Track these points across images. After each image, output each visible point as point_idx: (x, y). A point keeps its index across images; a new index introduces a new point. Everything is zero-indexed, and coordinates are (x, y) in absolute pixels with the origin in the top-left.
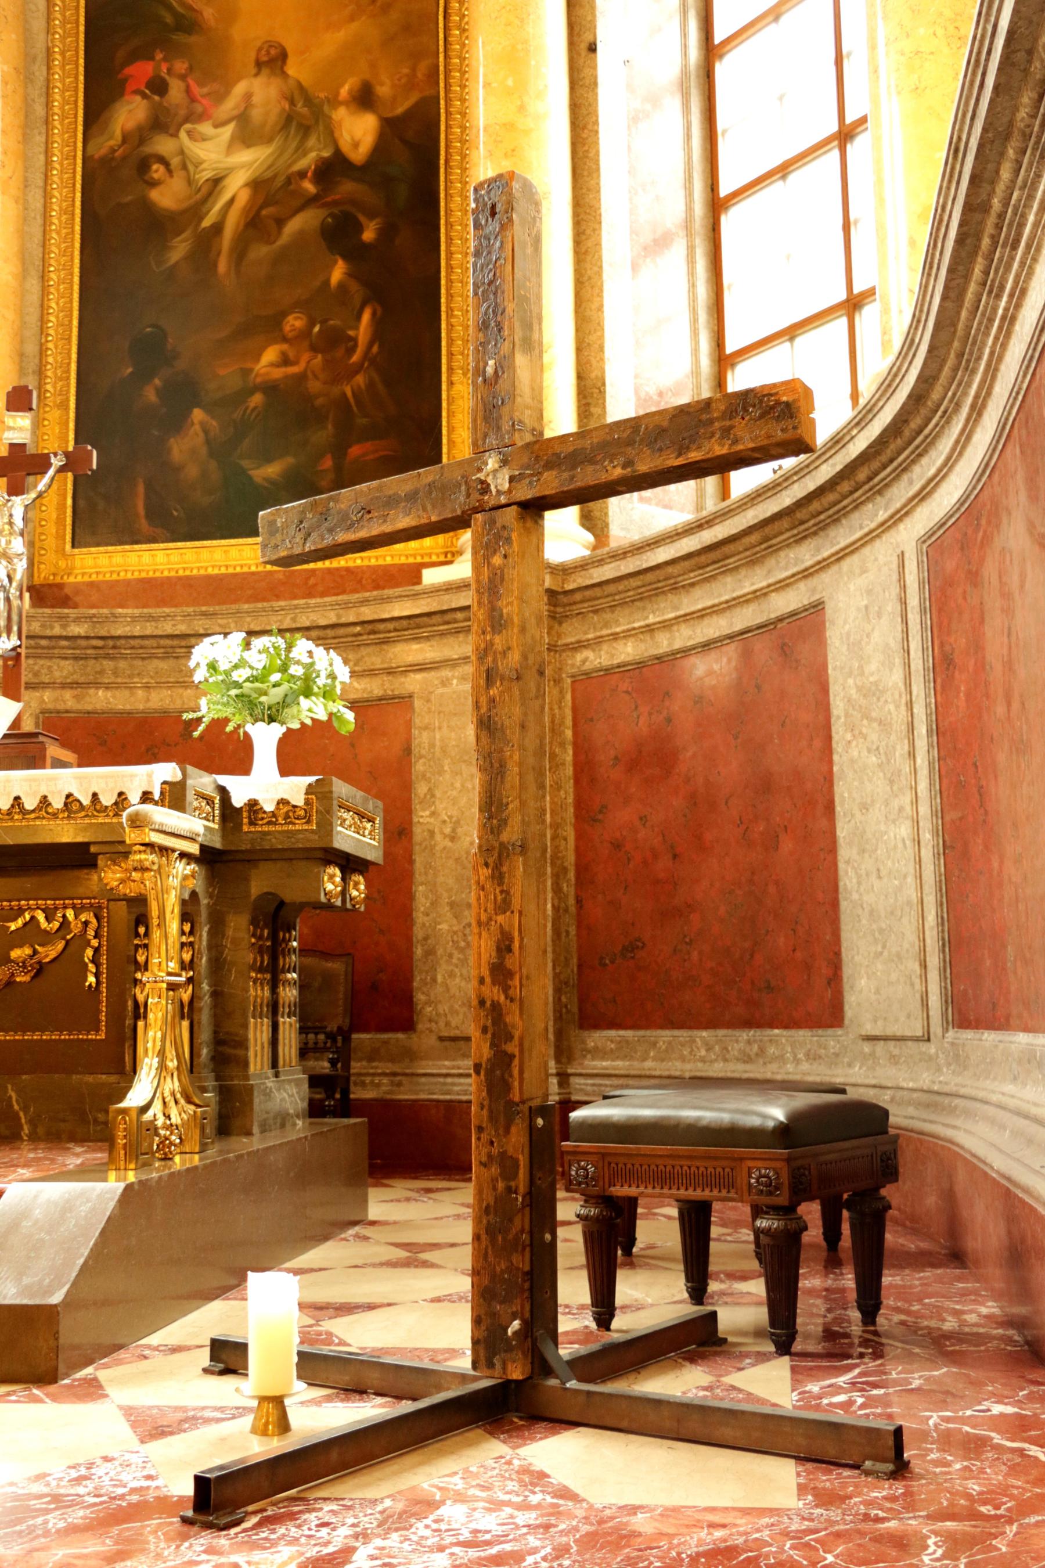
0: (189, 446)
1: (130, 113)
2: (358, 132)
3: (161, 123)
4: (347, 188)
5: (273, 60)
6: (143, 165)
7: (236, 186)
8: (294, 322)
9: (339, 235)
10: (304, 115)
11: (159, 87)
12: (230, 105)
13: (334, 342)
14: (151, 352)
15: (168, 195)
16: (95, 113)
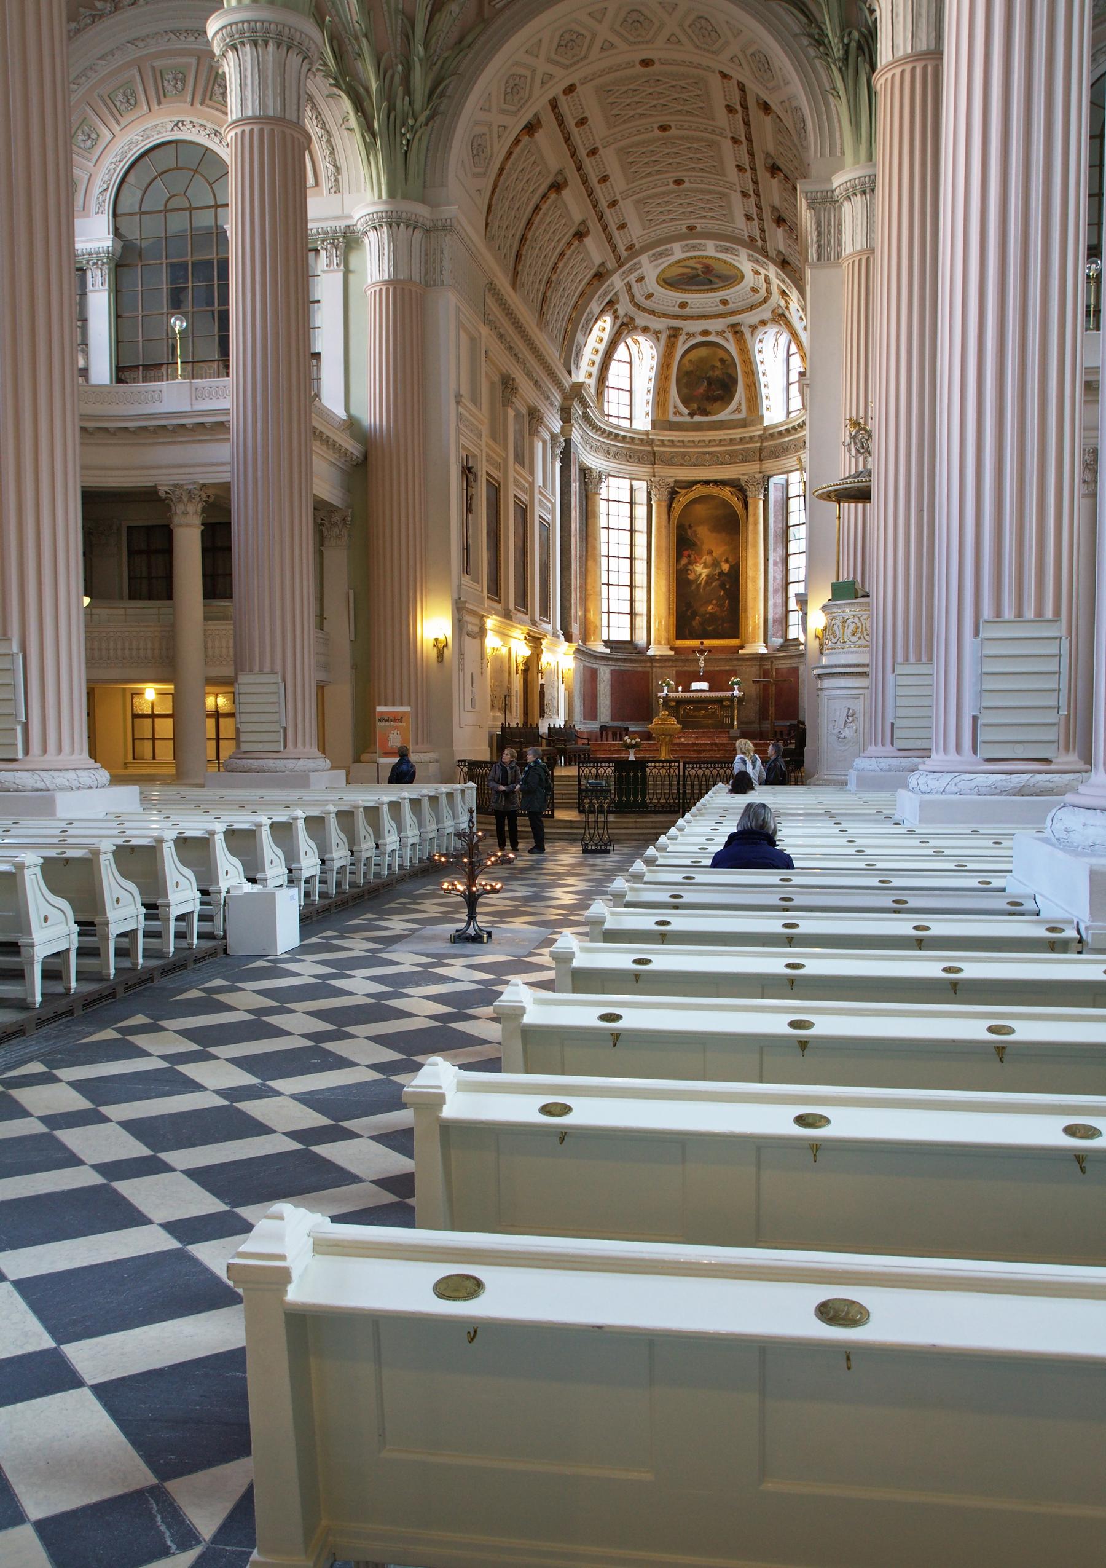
0: (696, 623)
1: (684, 561)
2: (726, 567)
3: (690, 563)
4: (724, 578)
5: (710, 553)
6: (687, 570)
7: (704, 575)
8: (714, 602)
9: (722, 586)
10: (715, 564)
11: (689, 556)
12: (703, 560)
13: (721, 606)
14: (689, 605)
15: (691, 577)
16: (678, 561)
